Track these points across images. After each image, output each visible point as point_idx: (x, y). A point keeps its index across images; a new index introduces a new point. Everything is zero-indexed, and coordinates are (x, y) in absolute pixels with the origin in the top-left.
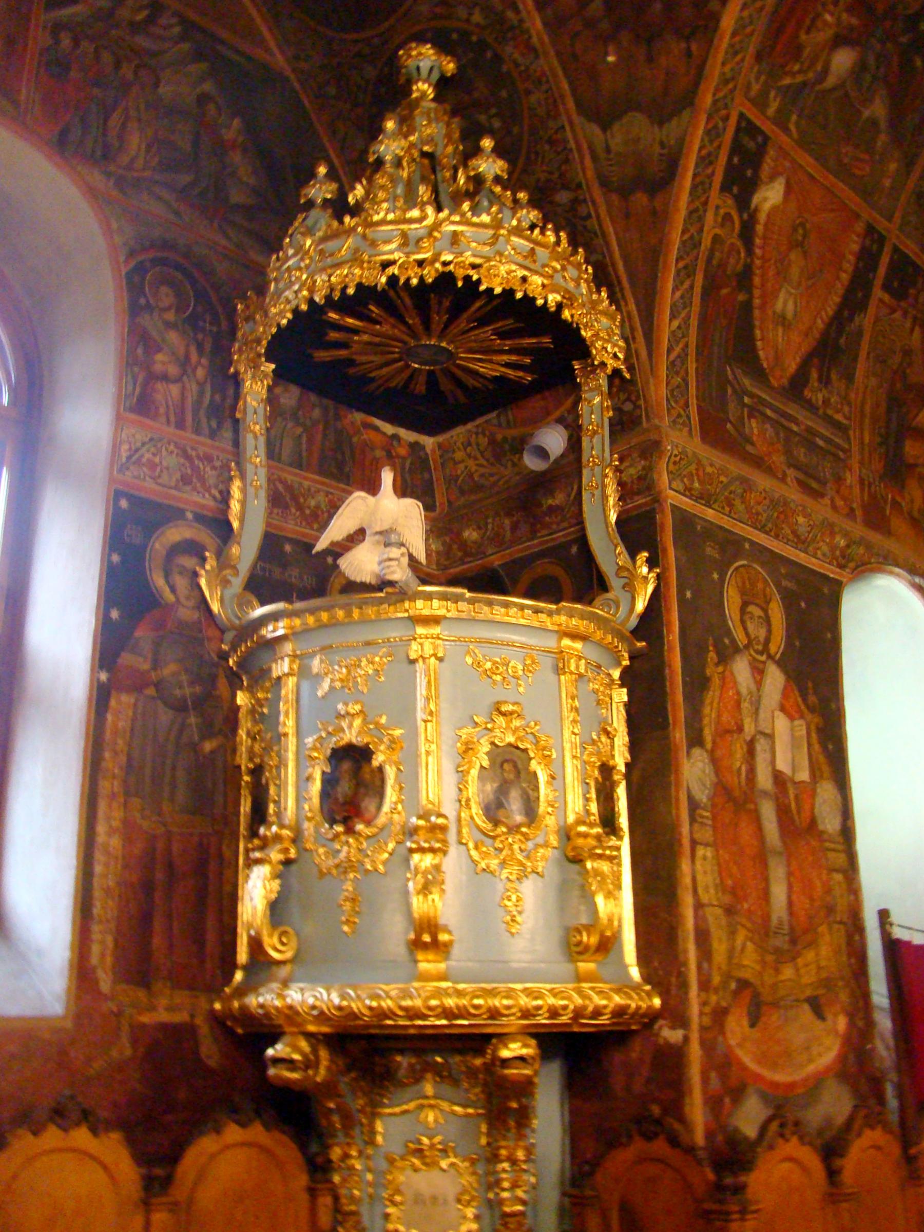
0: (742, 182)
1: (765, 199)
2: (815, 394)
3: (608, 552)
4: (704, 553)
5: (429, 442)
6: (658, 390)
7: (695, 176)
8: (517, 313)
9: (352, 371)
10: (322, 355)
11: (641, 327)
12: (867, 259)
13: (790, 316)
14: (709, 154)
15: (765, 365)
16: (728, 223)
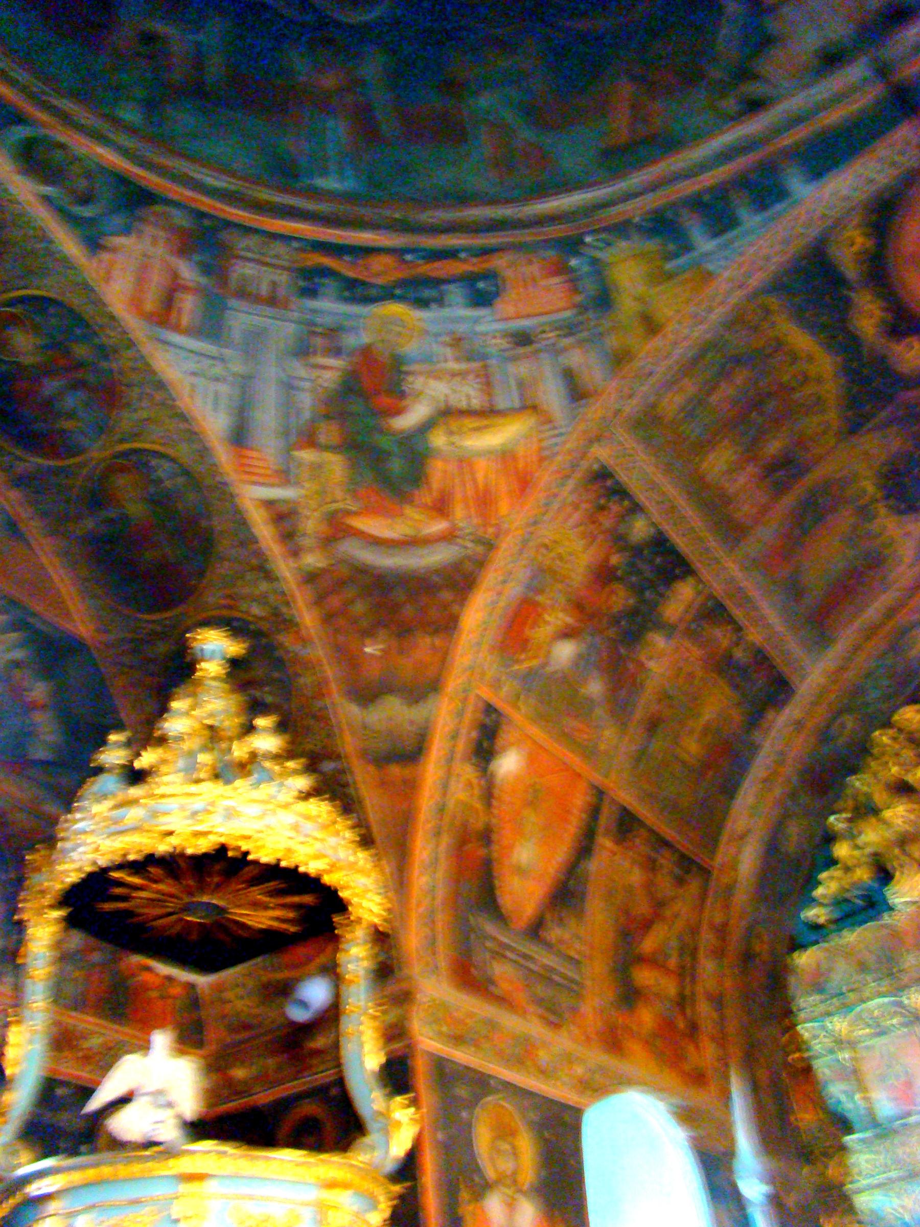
0: (484, 750)
2: (554, 933)
3: (369, 1097)
4: (458, 1092)
5: (202, 980)
6: (413, 941)
8: (286, 879)
9: (130, 920)
10: (108, 906)
11: (399, 883)
12: (594, 812)
13: (529, 863)
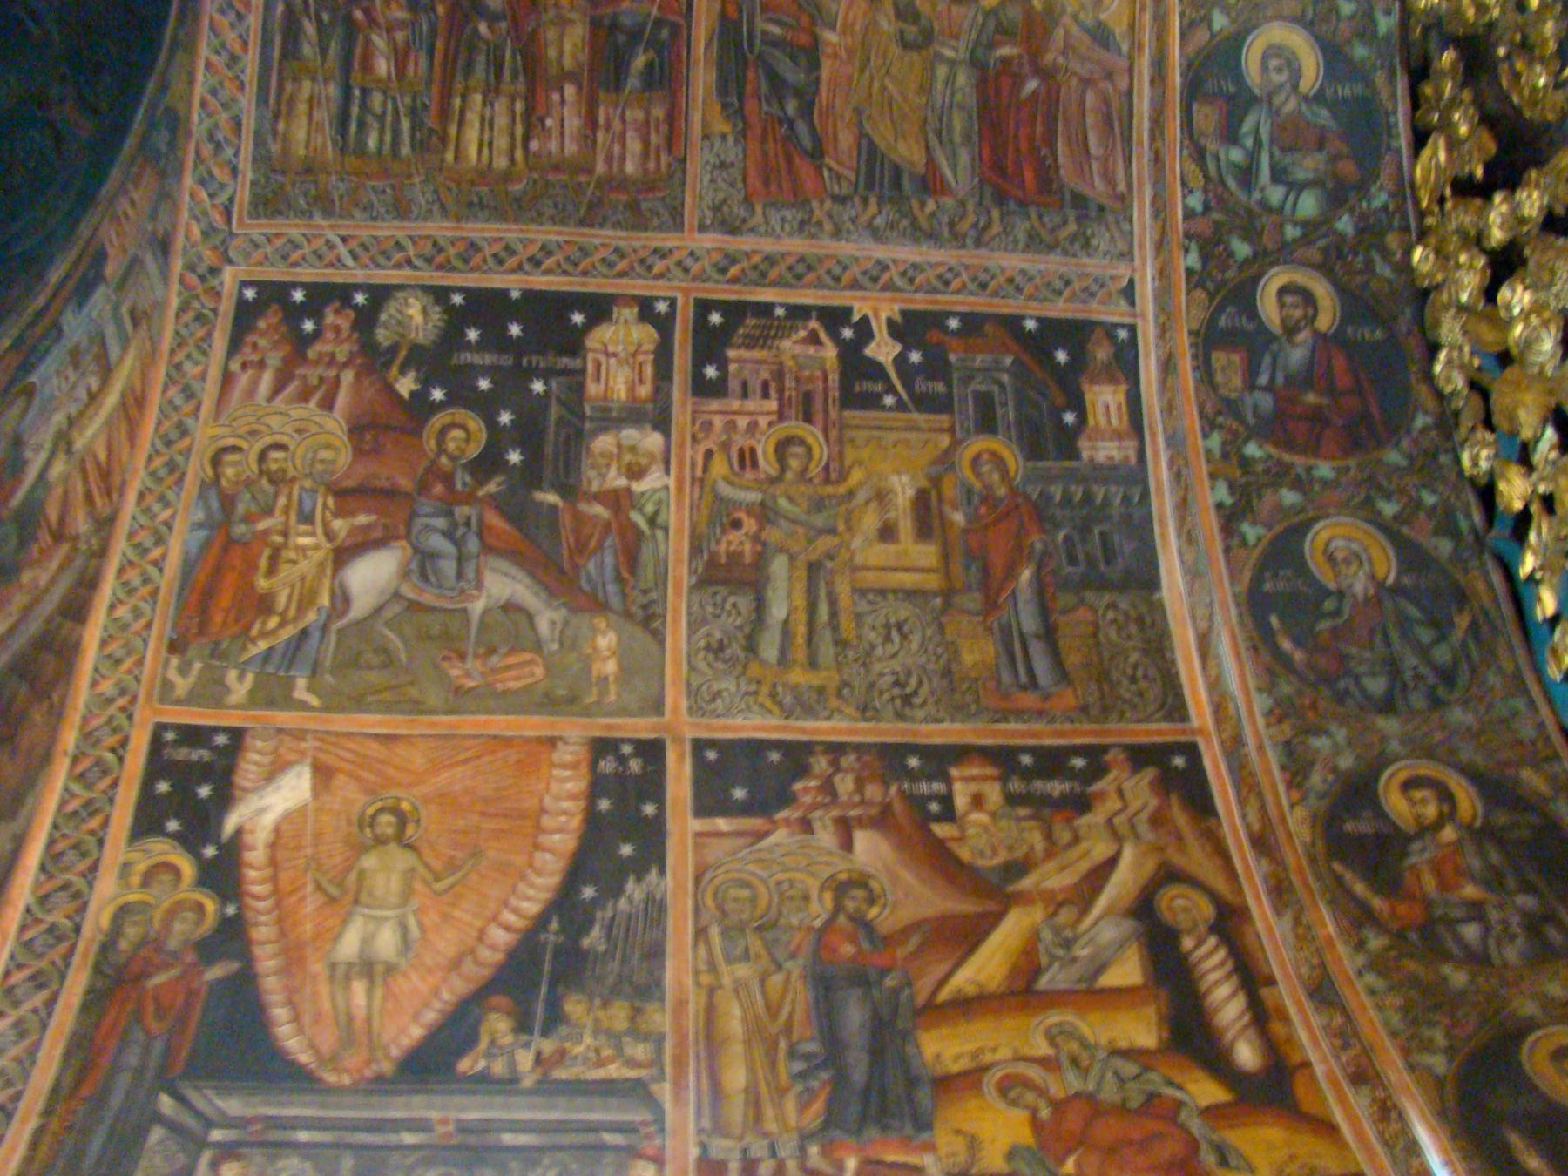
1: (262, 811)
7: (51, 842)
14: (88, 803)
15: (304, 1058)
16: (166, 877)
